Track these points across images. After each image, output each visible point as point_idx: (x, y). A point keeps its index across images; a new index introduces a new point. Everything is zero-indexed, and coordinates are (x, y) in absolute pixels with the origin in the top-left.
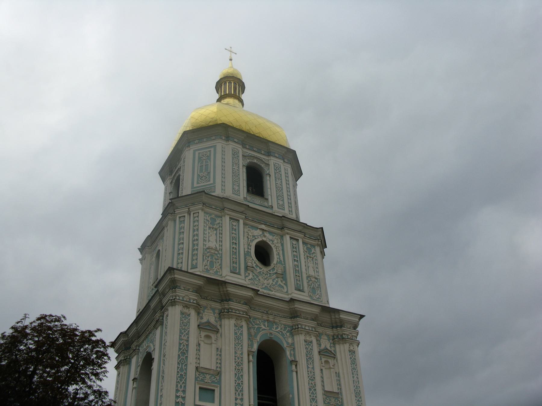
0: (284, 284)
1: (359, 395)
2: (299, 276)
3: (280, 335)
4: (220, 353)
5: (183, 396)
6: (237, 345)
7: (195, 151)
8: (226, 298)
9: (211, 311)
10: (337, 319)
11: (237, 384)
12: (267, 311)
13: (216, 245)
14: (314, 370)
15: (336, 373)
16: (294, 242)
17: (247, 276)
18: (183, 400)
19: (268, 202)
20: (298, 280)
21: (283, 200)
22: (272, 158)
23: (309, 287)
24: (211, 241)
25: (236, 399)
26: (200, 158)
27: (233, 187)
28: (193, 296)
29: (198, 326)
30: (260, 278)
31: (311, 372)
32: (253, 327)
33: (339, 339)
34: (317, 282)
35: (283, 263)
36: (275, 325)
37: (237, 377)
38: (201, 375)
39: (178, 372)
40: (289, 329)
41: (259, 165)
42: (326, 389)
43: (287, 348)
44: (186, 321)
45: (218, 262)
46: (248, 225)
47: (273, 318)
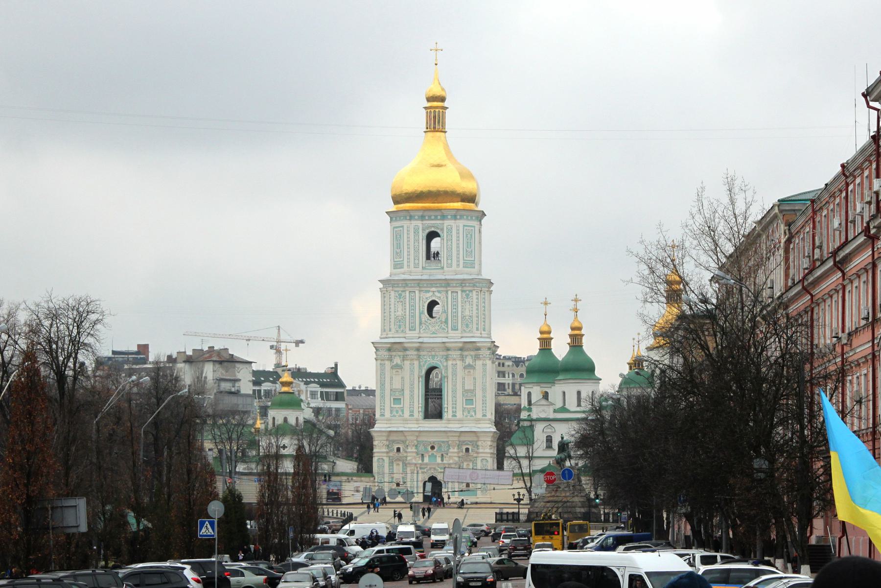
7: (394, 228)
8: (405, 349)
12: (432, 349)
16: (455, 295)
21: (451, 259)
22: (445, 222)
28: (384, 354)
33: (477, 358)
42: (466, 388)
46: (422, 291)
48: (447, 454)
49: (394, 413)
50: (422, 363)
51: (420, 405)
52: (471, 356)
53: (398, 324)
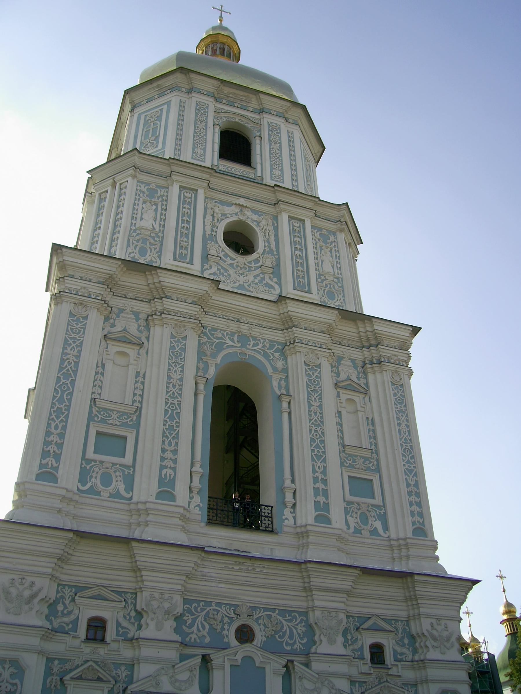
0: (275, 282)
1: (411, 453)
2: (302, 271)
3: (263, 356)
4: (143, 380)
5: (58, 442)
6: (173, 365)
7: (140, 116)
9: (133, 316)
10: (368, 333)
11: (167, 425)
13: (154, 224)
14: (321, 409)
15: (367, 418)
16: (297, 224)
17: (207, 269)
18: (58, 449)
19: (255, 174)
20: (301, 276)
21: (282, 170)
22: (265, 115)
23: (322, 289)
24: (145, 220)
25: (163, 451)
26: (146, 122)
27: (193, 149)
29: (105, 335)
30: (231, 271)
31: (316, 413)
32: (209, 342)
34: (337, 284)
35: (275, 253)
36: (251, 340)
37: (169, 414)
38: (102, 413)
39: (53, 403)
40: (280, 347)
41: (245, 126)
43: (274, 375)
44: (76, 326)
45: (155, 249)
47: (248, 328)
48: (307, 665)
49: (96, 482)
50: (208, 349)
51: (197, 468)
52: (353, 361)
53: (140, 244)
